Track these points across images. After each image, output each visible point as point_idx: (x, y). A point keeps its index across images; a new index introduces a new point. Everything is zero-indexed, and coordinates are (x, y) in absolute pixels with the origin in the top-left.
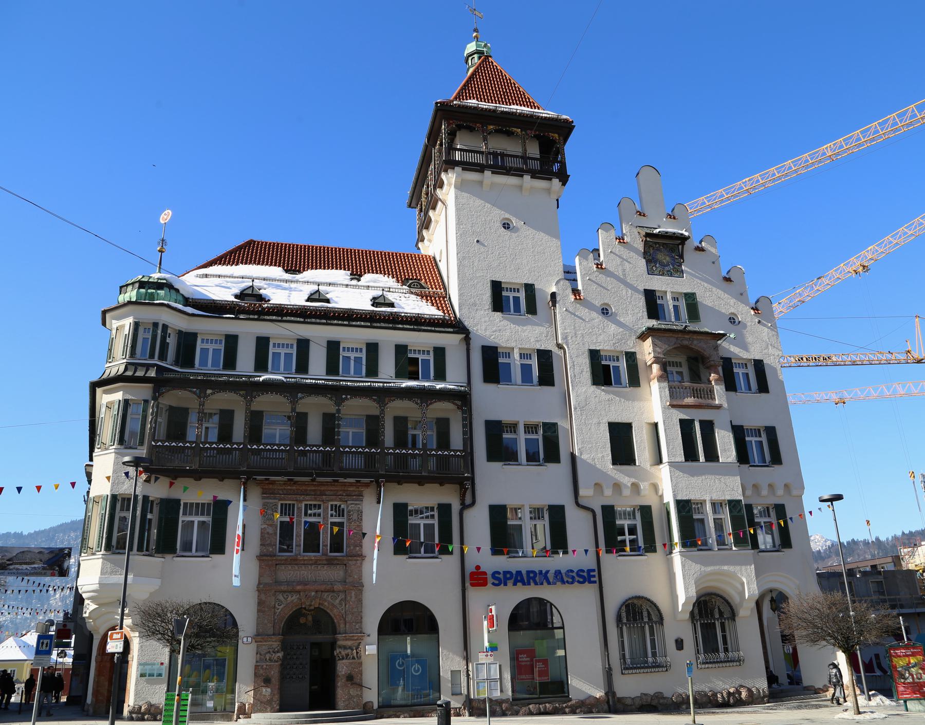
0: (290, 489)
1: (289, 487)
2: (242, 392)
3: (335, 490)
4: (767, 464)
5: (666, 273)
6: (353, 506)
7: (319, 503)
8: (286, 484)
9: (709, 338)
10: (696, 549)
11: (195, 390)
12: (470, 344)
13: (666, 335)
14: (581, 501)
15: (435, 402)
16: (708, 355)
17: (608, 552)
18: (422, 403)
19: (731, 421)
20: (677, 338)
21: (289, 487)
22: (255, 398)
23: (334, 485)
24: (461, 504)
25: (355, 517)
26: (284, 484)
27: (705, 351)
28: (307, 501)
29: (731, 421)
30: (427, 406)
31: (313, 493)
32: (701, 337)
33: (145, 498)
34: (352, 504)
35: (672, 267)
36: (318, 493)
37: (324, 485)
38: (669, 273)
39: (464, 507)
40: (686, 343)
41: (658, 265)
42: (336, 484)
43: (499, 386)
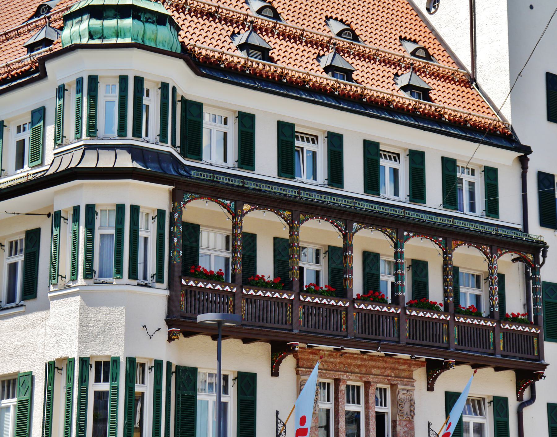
0: (332, 362)
1: (332, 360)
2: (287, 213)
3: (382, 368)
6: (405, 392)
7: (383, 386)
8: (332, 355)
11: (228, 202)
12: (527, 168)
18: (492, 254)
21: (332, 360)
22: (302, 223)
23: (386, 362)
24: (518, 399)
25: (406, 408)
26: (329, 355)
28: (352, 380)
30: (498, 257)
31: (357, 370)
33: (169, 364)
34: (403, 390)
36: (364, 370)
37: (375, 360)
39: (522, 405)
42: (389, 360)
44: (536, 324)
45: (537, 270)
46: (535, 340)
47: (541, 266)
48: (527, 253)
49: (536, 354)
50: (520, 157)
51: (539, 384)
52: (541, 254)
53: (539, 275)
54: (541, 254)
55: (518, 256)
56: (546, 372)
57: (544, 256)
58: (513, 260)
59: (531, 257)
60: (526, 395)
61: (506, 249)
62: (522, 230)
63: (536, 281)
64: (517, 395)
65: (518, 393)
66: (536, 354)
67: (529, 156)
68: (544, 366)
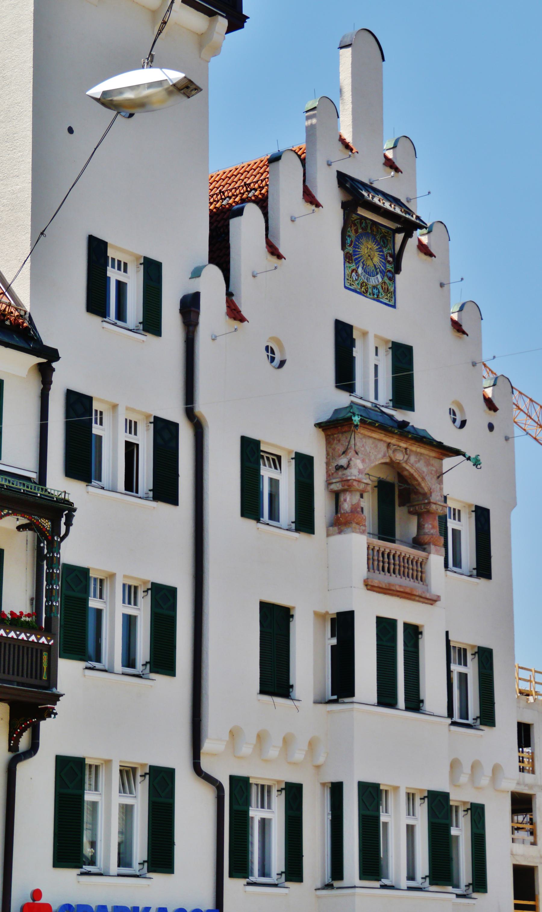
4: (470, 721)
5: (370, 290)
9: (433, 454)
10: (377, 884)
12: (51, 382)
13: (375, 435)
14: (206, 765)
15: (8, 514)
16: (426, 490)
17: (231, 876)
19: (447, 633)
20: (389, 445)
24: (11, 749)
27: (423, 479)
29: (447, 633)
32: (423, 451)
35: (380, 280)
38: (375, 291)
40: (399, 457)
41: (360, 270)
43: (90, 489)
44: (48, 631)
45: (55, 545)
46: (45, 656)
47: (63, 538)
48: (41, 517)
49: (45, 677)
50: (39, 364)
51: (44, 725)
52: (63, 520)
53: (58, 553)
54: (63, 520)
55: (28, 522)
56: (58, 707)
57: (68, 524)
58: (19, 528)
59: (47, 524)
60: (24, 742)
61: (9, 509)
62: (37, 481)
63: (53, 562)
64: (10, 743)
65: (10, 738)
66: (45, 677)
67: (54, 365)
68: (56, 698)
